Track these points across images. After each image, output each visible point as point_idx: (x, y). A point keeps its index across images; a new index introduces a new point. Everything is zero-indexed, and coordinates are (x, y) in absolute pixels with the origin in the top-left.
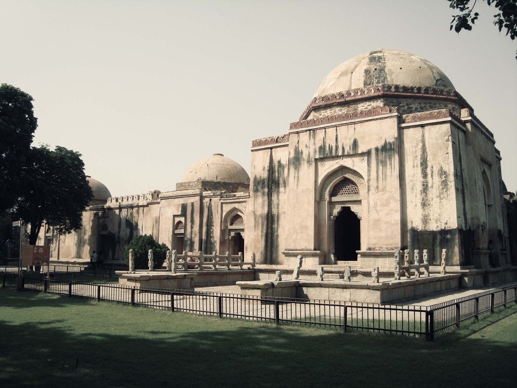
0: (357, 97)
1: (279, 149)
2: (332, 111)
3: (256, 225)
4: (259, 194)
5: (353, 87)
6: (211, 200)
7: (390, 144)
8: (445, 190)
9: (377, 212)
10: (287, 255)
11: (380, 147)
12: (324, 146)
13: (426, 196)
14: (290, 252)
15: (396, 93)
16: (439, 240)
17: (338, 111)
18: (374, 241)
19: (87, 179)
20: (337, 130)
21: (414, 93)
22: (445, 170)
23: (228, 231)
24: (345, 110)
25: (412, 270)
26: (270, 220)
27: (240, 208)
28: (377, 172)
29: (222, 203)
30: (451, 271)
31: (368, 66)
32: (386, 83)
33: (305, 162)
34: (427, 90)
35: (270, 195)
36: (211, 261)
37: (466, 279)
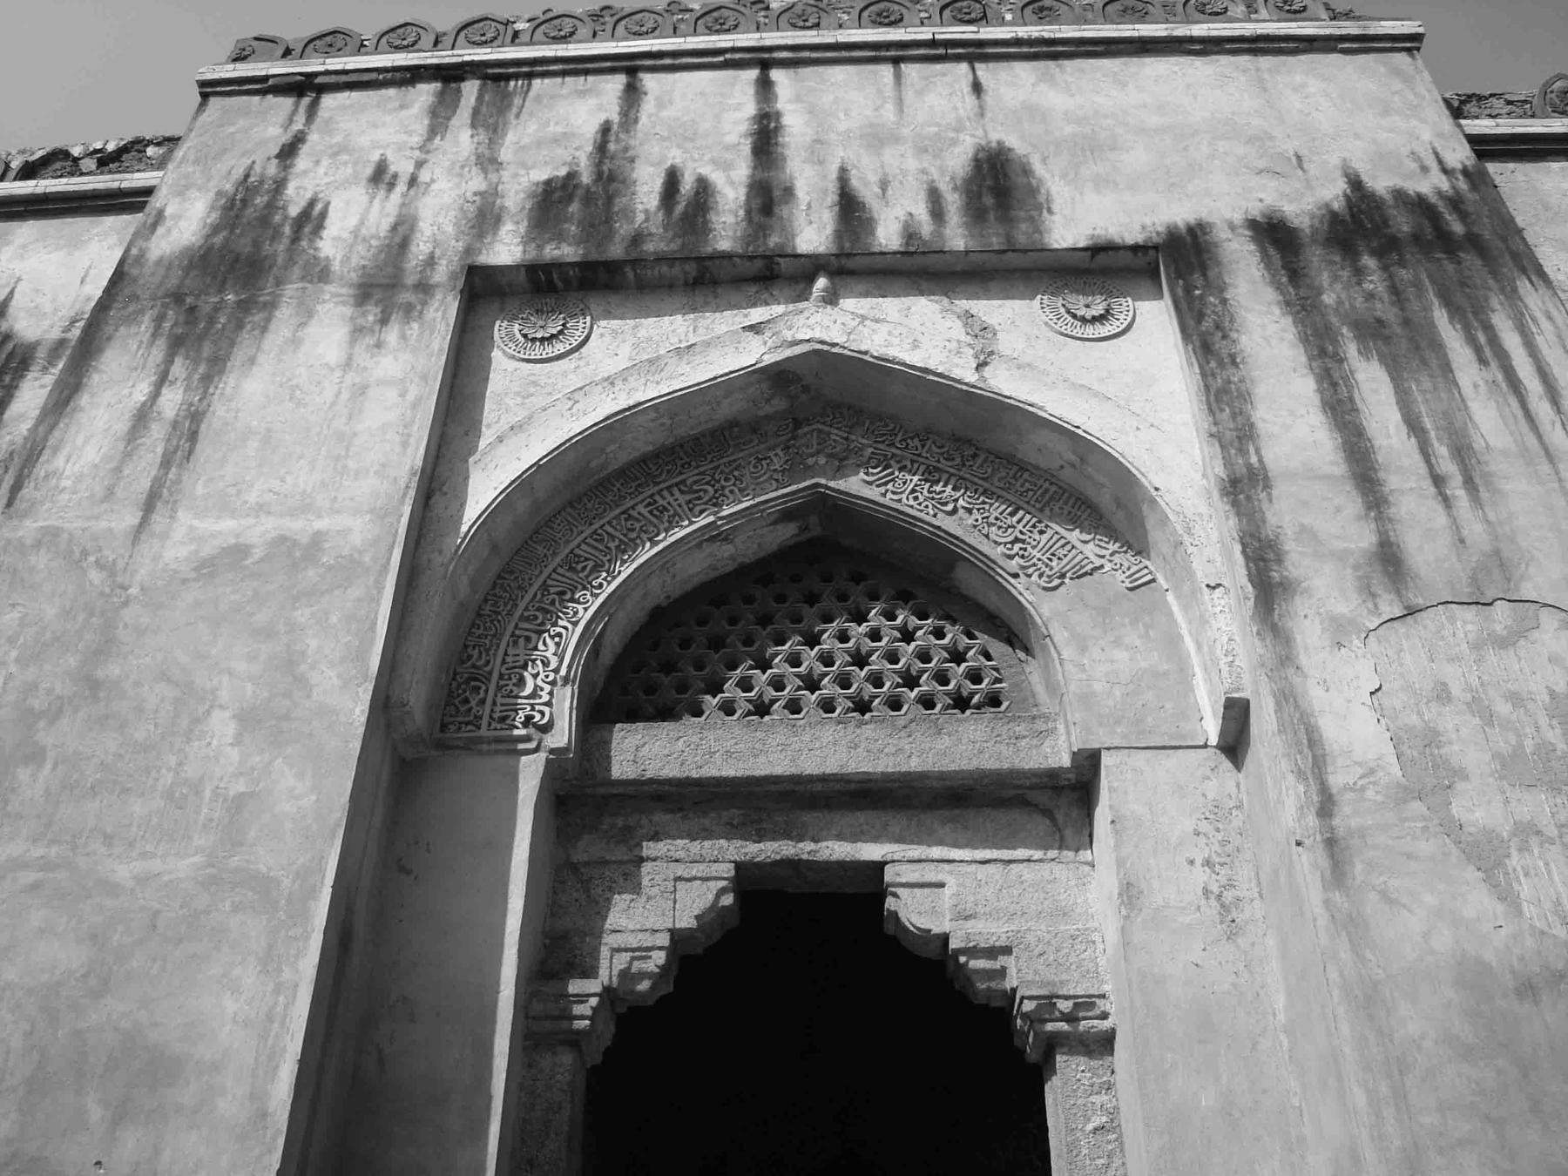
7: (1420, 206)
9: (1487, 856)
20: (765, 87)
28: (1340, 408)
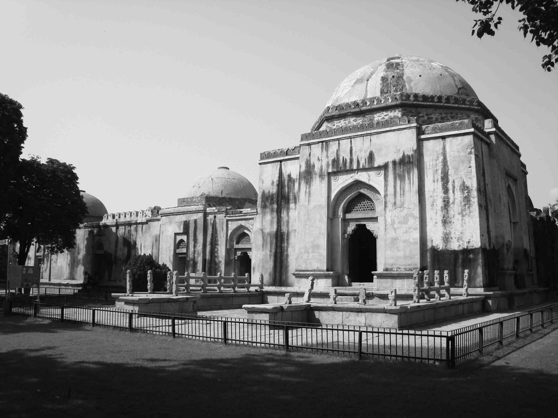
0: (373, 107)
1: (289, 162)
2: (347, 122)
3: (264, 244)
4: (268, 210)
5: (368, 97)
6: (215, 217)
7: (409, 157)
8: (467, 206)
9: (395, 230)
10: (298, 276)
11: (397, 161)
12: (338, 158)
13: (447, 213)
14: (301, 273)
15: (415, 102)
16: (461, 260)
17: (352, 121)
18: (391, 261)
19: (81, 193)
20: (351, 141)
21: (434, 102)
22: (468, 185)
23: (233, 250)
24: (359, 121)
25: (432, 293)
26: (279, 239)
27: (247, 226)
28: (395, 187)
29: (227, 221)
30: (474, 293)
31: (385, 73)
32: (404, 91)
33: (317, 176)
34: (448, 99)
35: (279, 212)
36: (215, 282)
37: (490, 302)
